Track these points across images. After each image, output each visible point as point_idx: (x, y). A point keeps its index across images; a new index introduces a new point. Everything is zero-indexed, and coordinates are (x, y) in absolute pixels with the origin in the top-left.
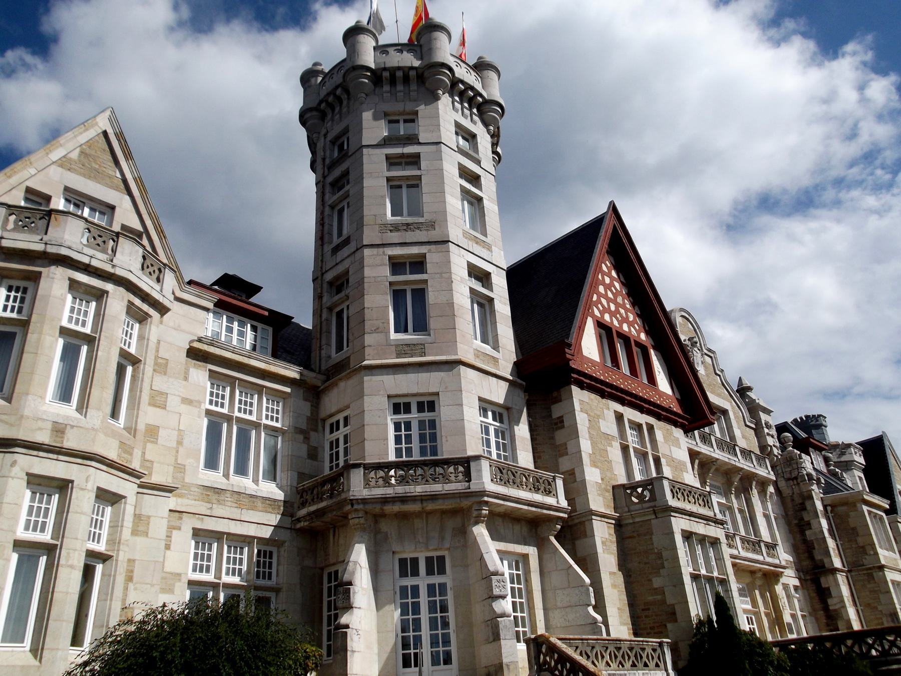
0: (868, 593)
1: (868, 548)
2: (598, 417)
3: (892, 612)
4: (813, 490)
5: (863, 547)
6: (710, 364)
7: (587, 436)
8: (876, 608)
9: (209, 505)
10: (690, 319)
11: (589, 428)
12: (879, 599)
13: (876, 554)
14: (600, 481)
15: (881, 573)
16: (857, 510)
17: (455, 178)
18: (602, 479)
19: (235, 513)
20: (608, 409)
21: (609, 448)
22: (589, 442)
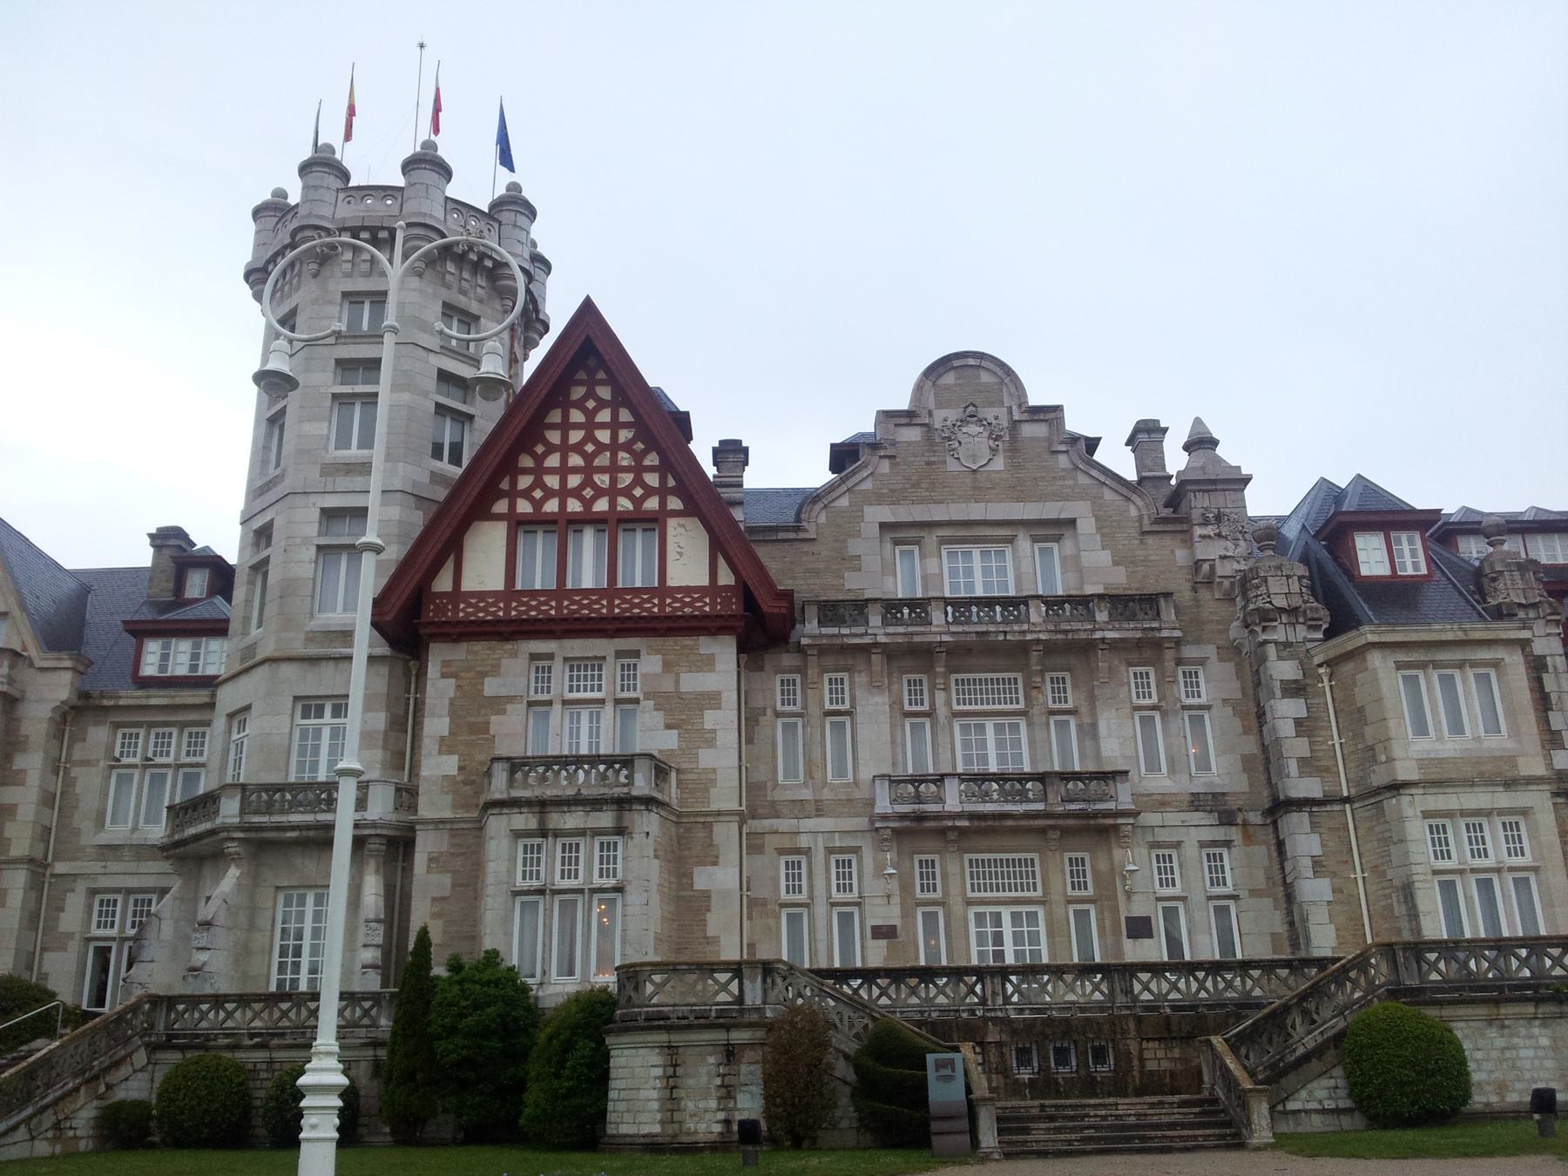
0: (1376, 843)
1: (1379, 748)
2: (484, 675)
3: (1406, 882)
4: (1276, 643)
5: (1372, 748)
6: (1032, 439)
7: (445, 711)
8: (1384, 874)
9: (104, 864)
10: (984, 364)
11: (452, 702)
12: (1389, 856)
13: (1390, 760)
14: (456, 773)
15: (1394, 801)
16: (1366, 669)
17: (322, 390)
18: (461, 769)
19: (131, 866)
20: (514, 655)
21: (493, 718)
22: (447, 720)
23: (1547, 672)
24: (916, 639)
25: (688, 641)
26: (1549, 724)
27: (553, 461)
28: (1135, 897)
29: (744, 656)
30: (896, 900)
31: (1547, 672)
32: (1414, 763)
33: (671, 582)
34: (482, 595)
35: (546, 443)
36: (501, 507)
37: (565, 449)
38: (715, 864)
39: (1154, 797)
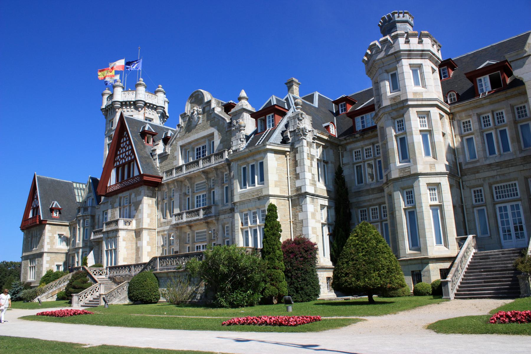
2: (114, 203)
23: (298, 153)
24: (179, 177)
25: (138, 189)
26: (296, 172)
27: (121, 152)
28: (218, 239)
29: (157, 189)
30: (178, 245)
31: (298, 153)
32: (239, 196)
33: (135, 175)
34: (113, 185)
35: (120, 147)
36: (115, 165)
37: (122, 148)
38: (140, 240)
39: (224, 210)
